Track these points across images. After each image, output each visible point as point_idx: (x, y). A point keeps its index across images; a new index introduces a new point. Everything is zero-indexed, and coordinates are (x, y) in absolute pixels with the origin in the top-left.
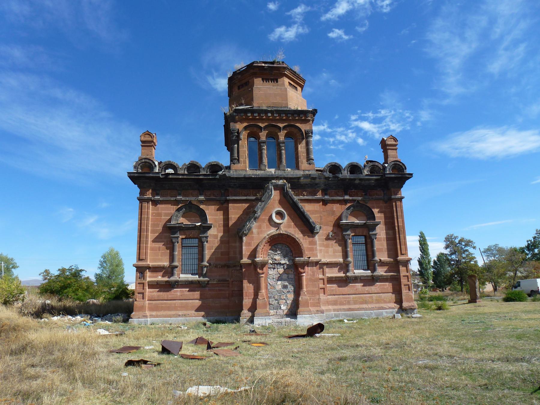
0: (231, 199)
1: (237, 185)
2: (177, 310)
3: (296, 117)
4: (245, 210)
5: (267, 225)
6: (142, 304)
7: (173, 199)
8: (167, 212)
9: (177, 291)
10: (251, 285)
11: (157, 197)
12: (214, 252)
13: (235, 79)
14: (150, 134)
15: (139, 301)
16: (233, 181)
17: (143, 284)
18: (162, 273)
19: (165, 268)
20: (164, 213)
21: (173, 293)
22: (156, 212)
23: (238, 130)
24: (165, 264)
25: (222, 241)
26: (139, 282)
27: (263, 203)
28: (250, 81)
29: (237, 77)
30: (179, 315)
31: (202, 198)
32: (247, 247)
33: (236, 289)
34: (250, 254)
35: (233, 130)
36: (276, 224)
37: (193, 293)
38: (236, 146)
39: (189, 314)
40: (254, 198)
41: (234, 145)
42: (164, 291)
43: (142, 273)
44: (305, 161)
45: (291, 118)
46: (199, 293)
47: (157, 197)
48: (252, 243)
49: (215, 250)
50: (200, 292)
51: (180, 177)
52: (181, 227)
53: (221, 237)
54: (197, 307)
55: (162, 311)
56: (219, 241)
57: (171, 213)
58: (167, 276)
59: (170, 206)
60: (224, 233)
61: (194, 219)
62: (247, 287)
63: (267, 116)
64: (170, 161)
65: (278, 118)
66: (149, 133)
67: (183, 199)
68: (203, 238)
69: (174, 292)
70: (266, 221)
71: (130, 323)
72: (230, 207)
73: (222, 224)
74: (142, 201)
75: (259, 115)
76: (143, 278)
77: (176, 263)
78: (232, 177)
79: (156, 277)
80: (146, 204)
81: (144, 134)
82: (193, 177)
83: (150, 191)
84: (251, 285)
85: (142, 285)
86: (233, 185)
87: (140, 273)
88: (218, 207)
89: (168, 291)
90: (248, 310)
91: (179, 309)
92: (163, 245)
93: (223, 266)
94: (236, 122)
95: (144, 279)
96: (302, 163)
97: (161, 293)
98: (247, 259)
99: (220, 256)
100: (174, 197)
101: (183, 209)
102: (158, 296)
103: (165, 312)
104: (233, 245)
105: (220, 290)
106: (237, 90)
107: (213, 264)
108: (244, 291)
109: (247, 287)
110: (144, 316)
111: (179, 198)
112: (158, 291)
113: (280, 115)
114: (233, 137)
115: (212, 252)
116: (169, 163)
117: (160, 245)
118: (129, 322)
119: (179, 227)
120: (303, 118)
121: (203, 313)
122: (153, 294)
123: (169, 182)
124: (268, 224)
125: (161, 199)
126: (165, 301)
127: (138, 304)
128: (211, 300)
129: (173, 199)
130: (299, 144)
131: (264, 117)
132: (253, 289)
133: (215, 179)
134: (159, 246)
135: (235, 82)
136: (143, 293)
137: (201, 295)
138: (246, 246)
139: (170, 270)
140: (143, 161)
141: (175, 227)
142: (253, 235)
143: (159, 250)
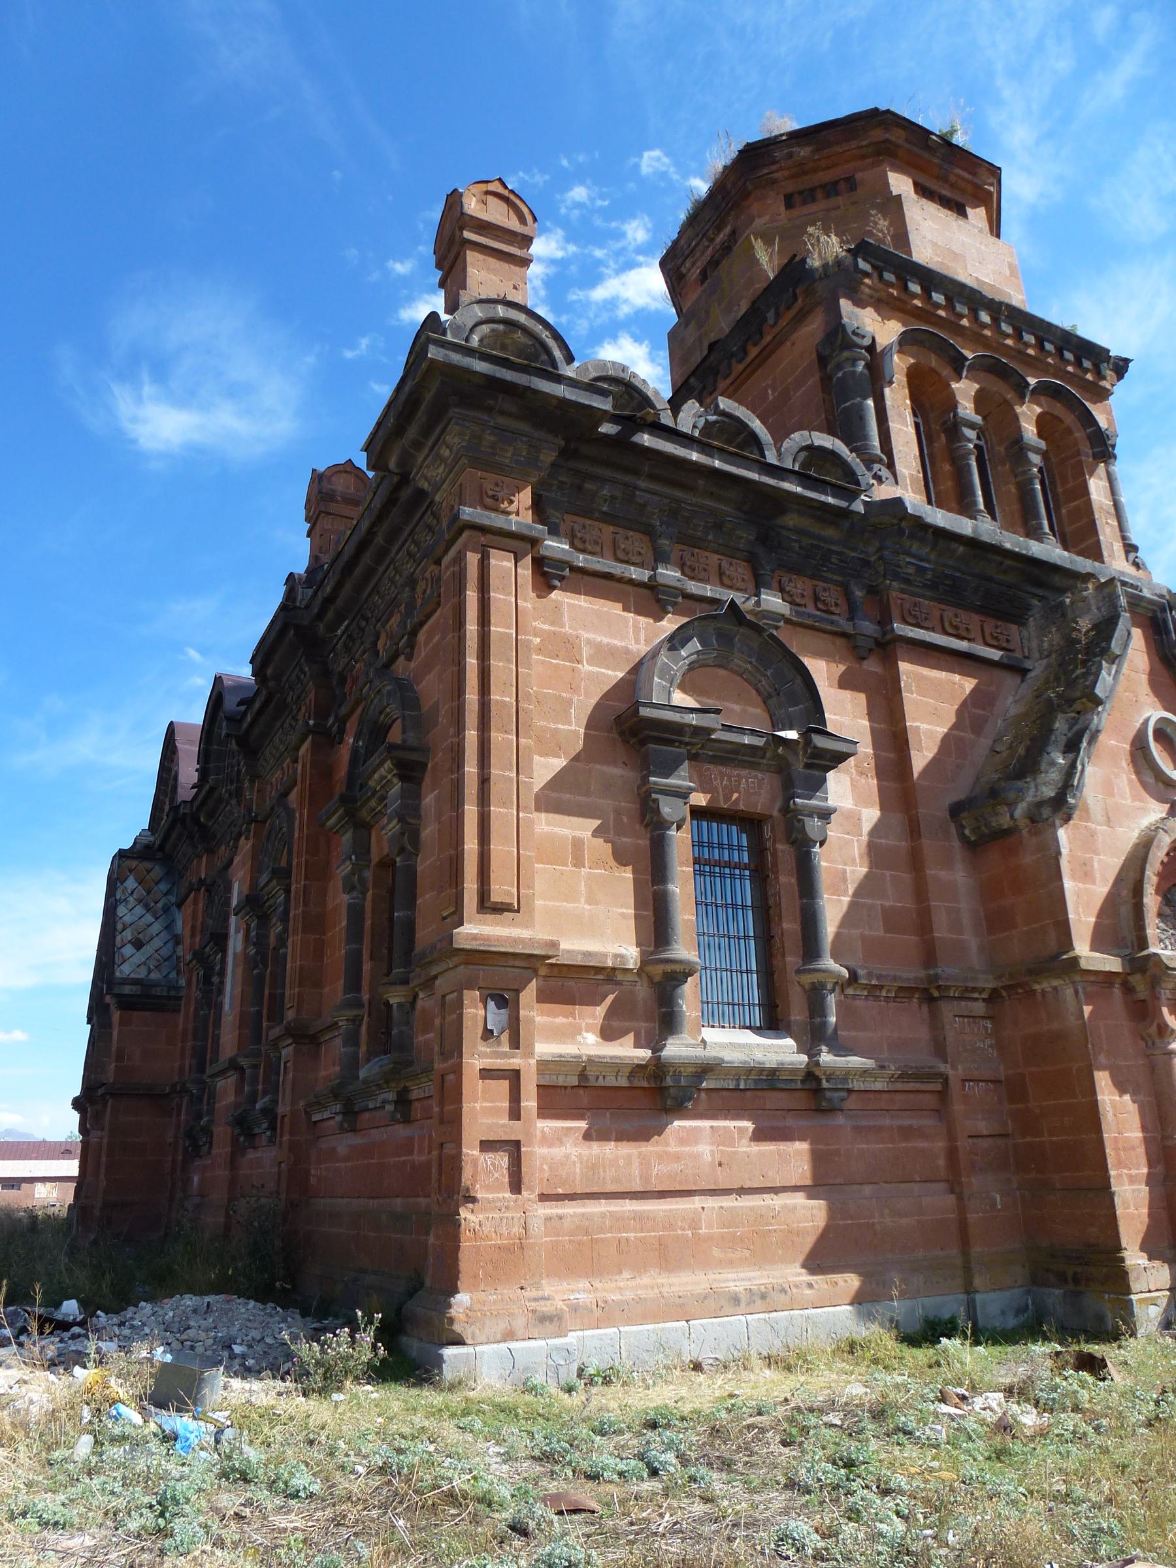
0: (911, 635)
1: (929, 575)
2: (707, 1264)
3: (1068, 363)
4: (964, 704)
5: (1130, 781)
6: (517, 1230)
7: (636, 573)
8: (606, 640)
9: (692, 1137)
10: (1127, 1097)
11: (556, 546)
12: (853, 905)
13: (775, 162)
14: (512, 197)
15: (492, 1205)
16: (915, 548)
17: (514, 1076)
18: (600, 1011)
19: (620, 977)
20: (589, 642)
21: (673, 1148)
22: (546, 627)
23: (873, 339)
24: (622, 951)
25: (876, 852)
26: (488, 1063)
27: (1114, 667)
28: (859, 176)
29: (790, 155)
30: (735, 1300)
31: (773, 601)
32: (1081, 885)
33: (983, 1127)
34: (1097, 925)
35: (854, 332)
36: (1161, 786)
37: (782, 1146)
38: (870, 402)
39: (783, 1291)
40: (995, 654)
41: (866, 398)
42: (622, 1137)
43: (502, 1002)
44: (1118, 547)
45: (1050, 360)
46: (802, 1147)
47: (556, 546)
48: (1096, 865)
49: (855, 894)
50: (811, 1144)
51: (695, 456)
52: (709, 731)
53: (874, 832)
54: (809, 1242)
55: (626, 1274)
56: (864, 849)
57: (627, 651)
58: (632, 1035)
59: (614, 609)
60: (881, 810)
61: (737, 707)
62: (1113, 1103)
63: (975, 319)
64: (624, 369)
65: (1009, 342)
66: (506, 193)
67: (693, 587)
68: (811, 816)
69: (682, 1141)
70: (1125, 763)
71: (452, 1388)
72: (903, 678)
73: (872, 762)
74: (483, 540)
75: (950, 305)
76: (505, 1037)
77: (684, 950)
78: (929, 520)
79: (570, 1034)
80: (509, 561)
81: (483, 187)
82: (754, 476)
83: (525, 497)
84: (1127, 1097)
85: (505, 1084)
86: (911, 570)
87: (491, 1004)
88: (842, 668)
89: (647, 1138)
90: (1143, 1248)
91: (716, 1252)
92: (597, 833)
93: (905, 992)
94: (860, 303)
95: (515, 1043)
96: (1112, 556)
97: (609, 1150)
98: (1091, 950)
99: (881, 933)
100: (641, 565)
101: (689, 639)
102: (593, 1167)
103: (645, 1280)
104: (943, 874)
105: (906, 1133)
106: (782, 209)
107: (870, 975)
108: (1105, 1135)
109: (1113, 1103)
110: (544, 1319)
111: (669, 574)
112: (587, 1136)
113: (1018, 336)
114: (854, 361)
115: (845, 908)
116: (622, 375)
117: (582, 828)
118: (448, 1373)
119: (697, 731)
120: (1089, 377)
121: (851, 1282)
122: (558, 1152)
123: (619, 476)
124: (1134, 777)
125: (581, 560)
126: (629, 1206)
127: (487, 1229)
128: (867, 1190)
129: (636, 573)
130: (1091, 476)
131: (965, 322)
132: (1136, 1121)
133: (846, 513)
134: (578, 833)
135: (776, 175)
136: (517, 1144)
137: (819, 1159)
138: (1073, 877)
139: (642, 991)
140: (501, 311)
141: (678, 729)
142: (1093, 826)
143: (578, 862)
